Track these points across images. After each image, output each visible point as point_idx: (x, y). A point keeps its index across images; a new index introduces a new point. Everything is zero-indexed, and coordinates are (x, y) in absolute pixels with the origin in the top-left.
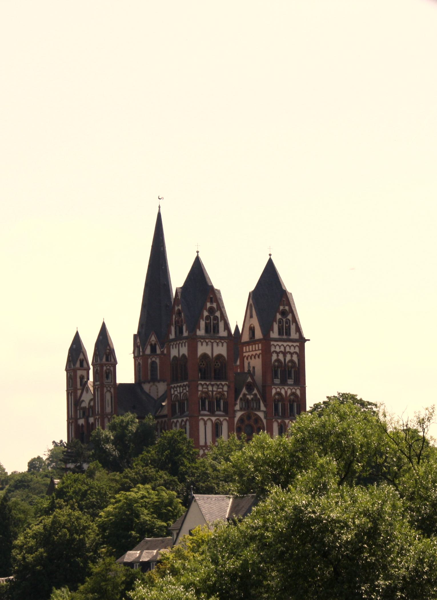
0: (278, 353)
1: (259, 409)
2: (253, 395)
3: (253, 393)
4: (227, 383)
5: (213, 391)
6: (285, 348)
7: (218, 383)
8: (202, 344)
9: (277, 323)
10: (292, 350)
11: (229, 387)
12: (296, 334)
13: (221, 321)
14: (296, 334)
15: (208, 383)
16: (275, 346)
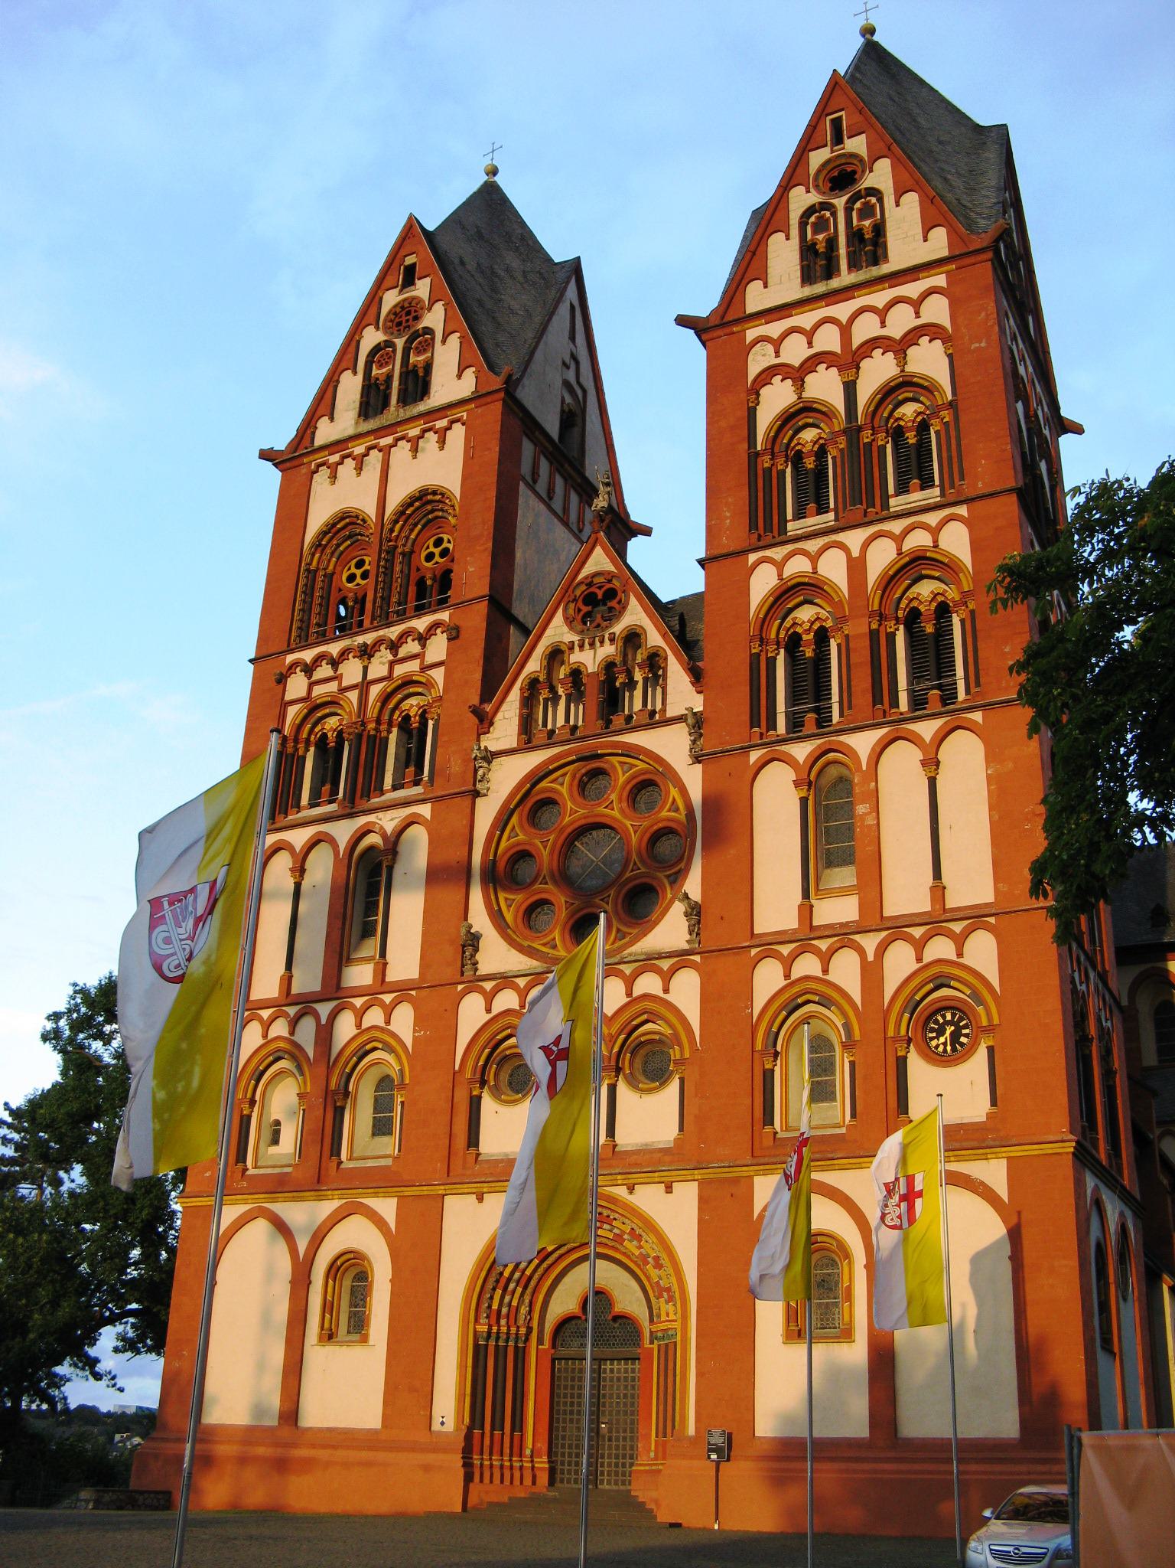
0: (798, 375)
1: (654, 720)
2: (612, 640)
3: (618, 628)
4: (444, 616)
5: (364, 686)
6: (846, 330)
7: (393, 632)
8: (333, 477)
9: (794, 231)
10: (901, 321)
11: (454, 634)
12: (925, 239)
13: (444, 342)
14: (925, 239)
15: (334, 649)
16: (777, 344)
